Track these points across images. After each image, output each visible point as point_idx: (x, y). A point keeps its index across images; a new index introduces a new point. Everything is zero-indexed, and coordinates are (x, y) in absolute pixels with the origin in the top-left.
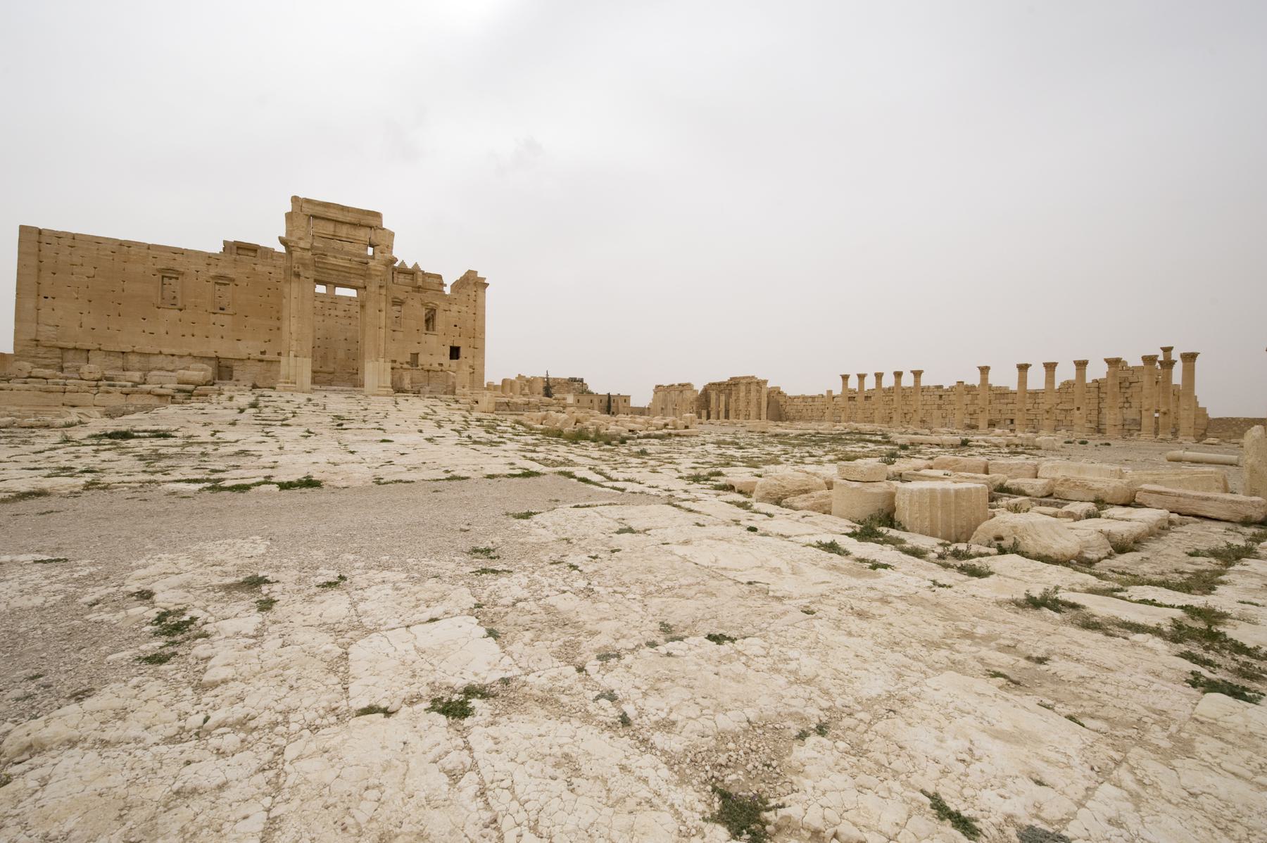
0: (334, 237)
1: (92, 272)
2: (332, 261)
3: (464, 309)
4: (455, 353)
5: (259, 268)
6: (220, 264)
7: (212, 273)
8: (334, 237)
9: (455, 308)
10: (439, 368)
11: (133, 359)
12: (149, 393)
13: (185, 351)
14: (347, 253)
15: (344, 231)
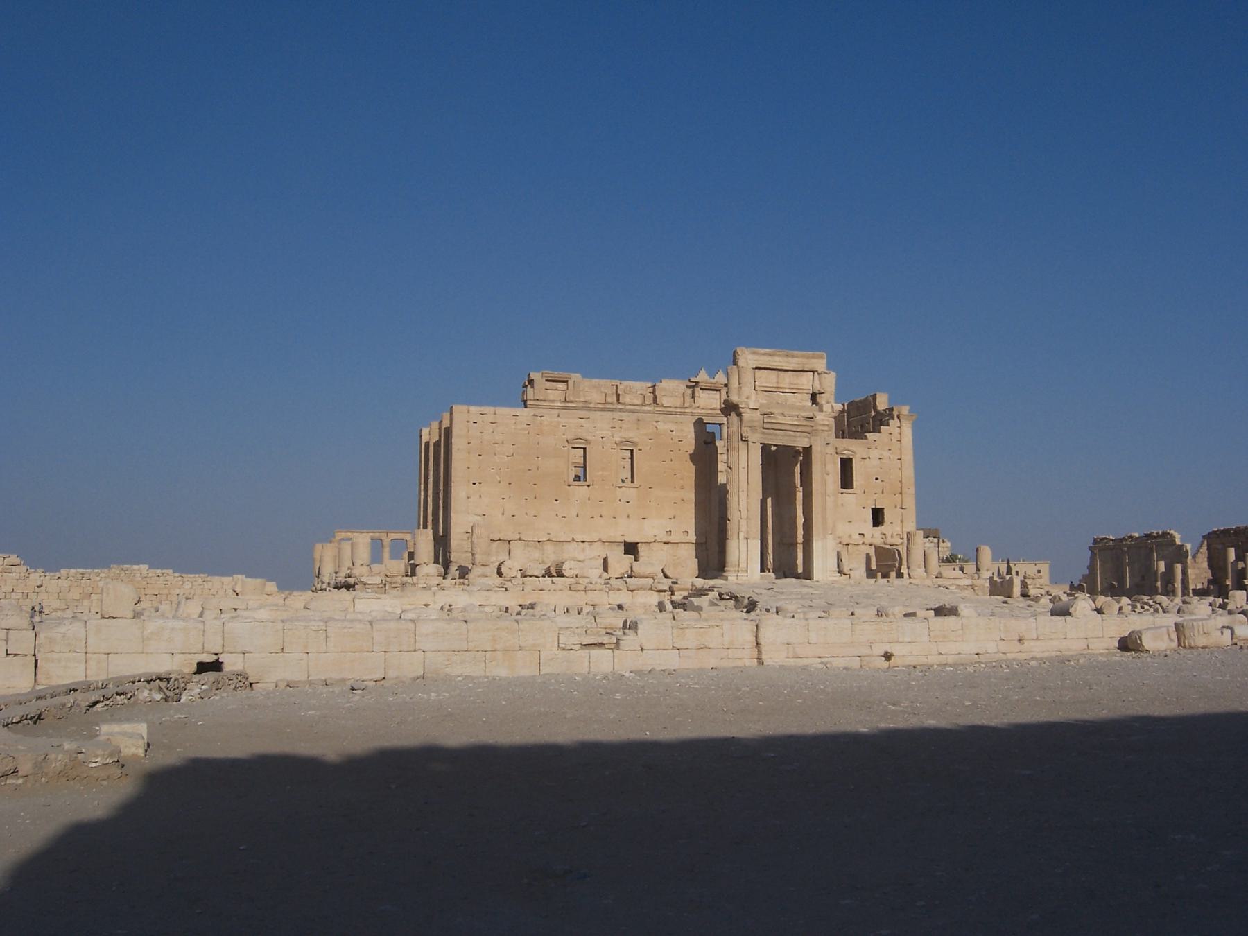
0: (779, 390)
1: (511, 450)
2: (781, 420)
3: (886, 454)
4: (878, 517)
5: (661, 426)
6: (624, 426)
7: (618, 439)
8: (779, 390)
9: (874, 454)
10: (859, 540)
11: (549, 548)
12: (651, 589)
13: (595, 537)
14: (792, 407)
15: (787, 380)
